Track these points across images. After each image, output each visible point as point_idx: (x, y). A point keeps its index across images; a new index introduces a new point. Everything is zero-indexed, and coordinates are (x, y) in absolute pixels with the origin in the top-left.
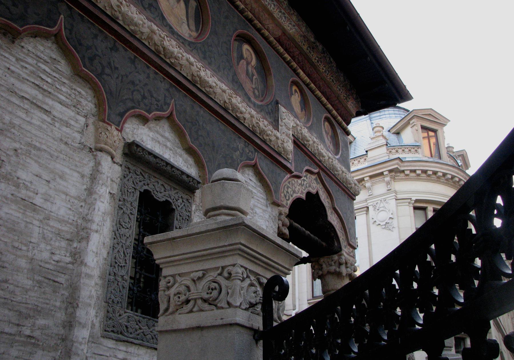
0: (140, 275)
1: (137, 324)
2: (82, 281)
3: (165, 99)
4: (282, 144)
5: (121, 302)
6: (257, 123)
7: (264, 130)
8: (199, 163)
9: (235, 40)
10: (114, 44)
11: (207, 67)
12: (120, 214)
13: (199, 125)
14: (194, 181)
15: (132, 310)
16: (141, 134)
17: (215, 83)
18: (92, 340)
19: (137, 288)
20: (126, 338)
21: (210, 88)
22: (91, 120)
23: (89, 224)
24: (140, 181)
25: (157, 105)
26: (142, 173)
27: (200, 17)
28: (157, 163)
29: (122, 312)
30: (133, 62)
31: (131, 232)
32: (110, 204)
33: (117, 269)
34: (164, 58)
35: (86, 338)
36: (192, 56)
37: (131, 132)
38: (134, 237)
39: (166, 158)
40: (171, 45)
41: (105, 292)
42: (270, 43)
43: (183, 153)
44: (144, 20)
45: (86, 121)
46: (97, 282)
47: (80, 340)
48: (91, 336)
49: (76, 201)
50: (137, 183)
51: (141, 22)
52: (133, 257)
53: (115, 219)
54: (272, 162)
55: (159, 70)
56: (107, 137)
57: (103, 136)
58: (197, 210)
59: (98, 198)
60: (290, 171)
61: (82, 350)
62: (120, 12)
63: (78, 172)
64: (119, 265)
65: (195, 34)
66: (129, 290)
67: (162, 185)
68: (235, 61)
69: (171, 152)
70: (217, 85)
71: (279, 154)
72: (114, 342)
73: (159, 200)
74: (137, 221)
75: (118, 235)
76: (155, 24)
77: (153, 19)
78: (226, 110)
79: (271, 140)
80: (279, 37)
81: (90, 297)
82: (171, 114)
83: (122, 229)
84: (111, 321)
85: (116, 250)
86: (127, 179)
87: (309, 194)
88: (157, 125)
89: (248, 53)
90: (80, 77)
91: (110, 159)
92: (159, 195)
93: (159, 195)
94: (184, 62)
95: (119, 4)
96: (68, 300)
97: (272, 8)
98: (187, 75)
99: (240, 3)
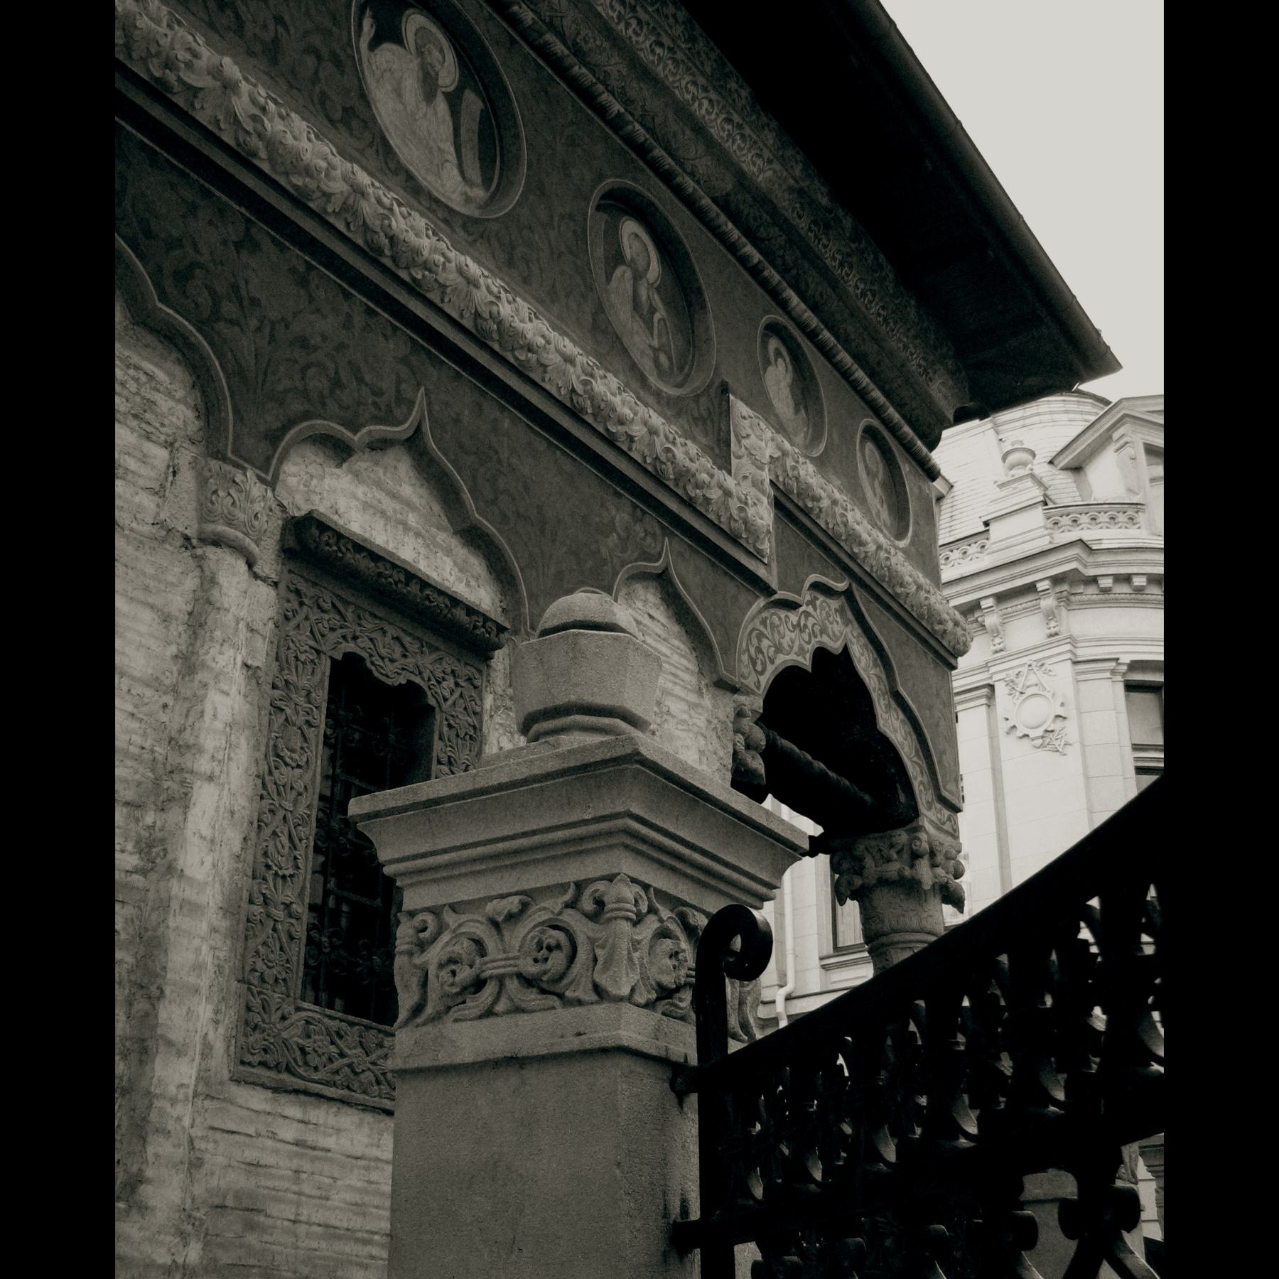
0: (339, 901)
1: (332, 1043)
2: (172, 922)
3: (398, 391)
4: (741, 509)
5: (284, 980)
6: (668, 450)
7: (688, 471)
9: (599, 208)
10: (248, 230)
11: (518, 289)
12: (275, 727)
13: (499, 461)
14: (489, 624)
15: (316, 1003)
16: (334, 491)
17: (543, 336)
18: (207, 1090)
19: (330, 938)
20: (300, 1084)
21: (530, 350)
22: (186, 456)
23: (188, 756)
24: (332, 629)
25: (375, 404)
26: (339, 605)
27: (492, 144)
28: (380, 574)
29: (288, 1008)
30: (303, 282)
31: (308, 776)
32: (245, 696)
33: (271, 883)
34: (393, 268)
35: (188, 1086)
36: (475, 260)
37: (302, 487)
38: (317, 791)
39: (404, 561)
40: (412, 228)
41: (240, 951)
42: (700, 214)
43: (455, 543)
44: (330, 157)
45: (172, 458)
46: (216, 923)
47: (172, 1090)
48: (203, 1078)
49: (148, 692)
50: (323, 636)
51: (323, 164)
52: (317, 850)
53: (264, 741)
54: (713, 564)
55: (377, 303)
56: (234, 503)
57: (223, 501)
58: (498, 708)
59: (212, 683)
60: (766, 590)
61: (179, 1119)
62: (260, 136)
63: (152, 607)
64: (276, 874)
65: (479, 193)
66: (307, 945)
68: (599, 270)
69: (420, 540)
70: (548, 342)
71: (734, 540)
72: (269, 1094)
73: (389, 682)
74: (325, 744)
75: (271, 787)
76: (364, 168)
77: (357, 154)
78: (575, 414)
79: (707, 501)
80: (728, 195)
81: (198, 967)
82: (418, 430)
83: (284, 769)
84: (257, 1035)
85: (267, 832)
86: (293, 623)
88: (377, 464)
89: (636, 245)
90: (152, 330)
91: (242, 566)
92: (389, 668)
93: (389, 668)
94: (450, 277)
95: (257, 112)
96: (133, 978)
97: (703, 112)
98: (462, 316)
99: (611, 98)
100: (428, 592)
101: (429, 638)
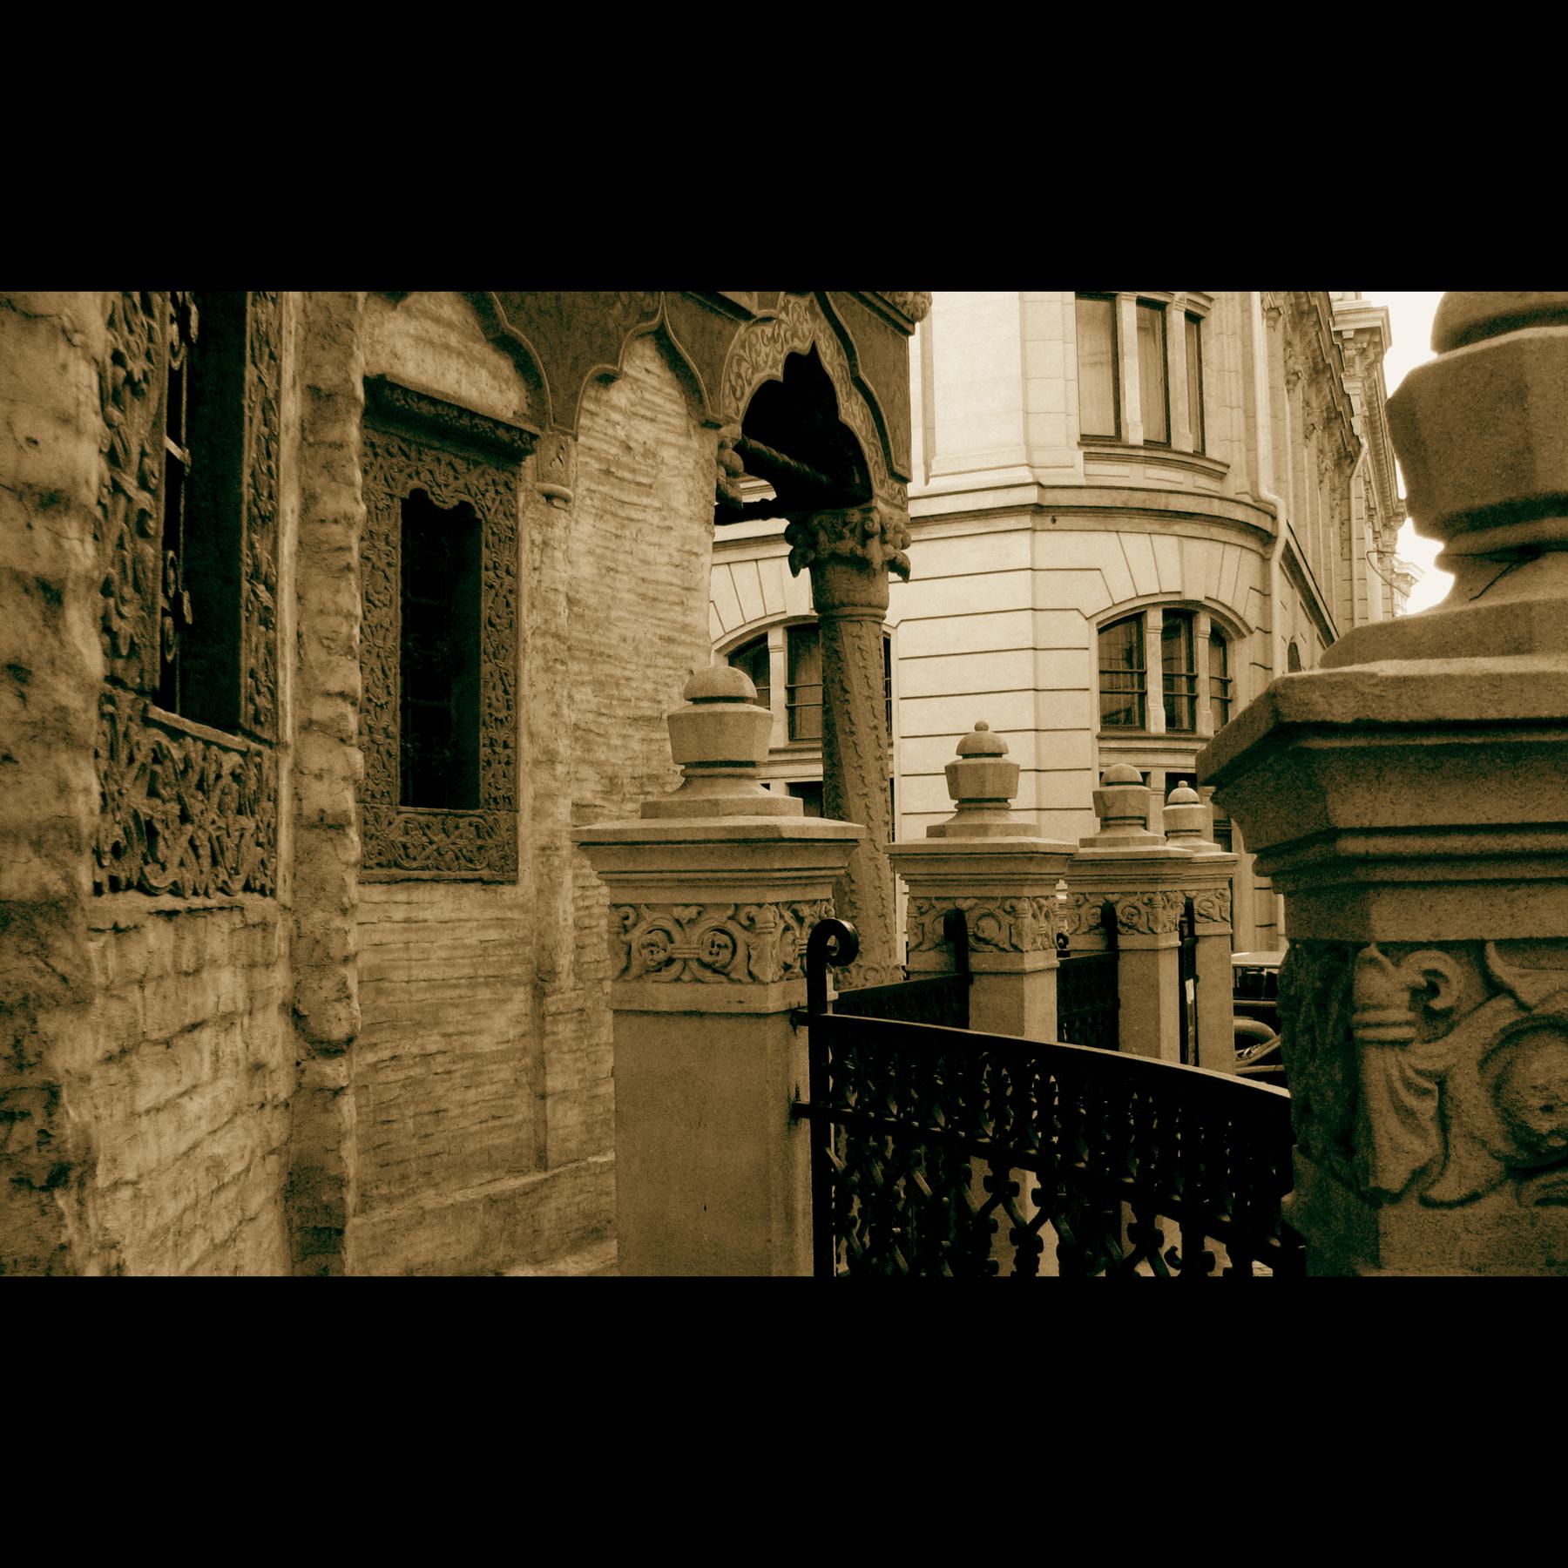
8: (525, 368)
31: (391, 613)
67: (450, 464)
73: (446, 507)
93: (445, 492)
101: (474, 455)
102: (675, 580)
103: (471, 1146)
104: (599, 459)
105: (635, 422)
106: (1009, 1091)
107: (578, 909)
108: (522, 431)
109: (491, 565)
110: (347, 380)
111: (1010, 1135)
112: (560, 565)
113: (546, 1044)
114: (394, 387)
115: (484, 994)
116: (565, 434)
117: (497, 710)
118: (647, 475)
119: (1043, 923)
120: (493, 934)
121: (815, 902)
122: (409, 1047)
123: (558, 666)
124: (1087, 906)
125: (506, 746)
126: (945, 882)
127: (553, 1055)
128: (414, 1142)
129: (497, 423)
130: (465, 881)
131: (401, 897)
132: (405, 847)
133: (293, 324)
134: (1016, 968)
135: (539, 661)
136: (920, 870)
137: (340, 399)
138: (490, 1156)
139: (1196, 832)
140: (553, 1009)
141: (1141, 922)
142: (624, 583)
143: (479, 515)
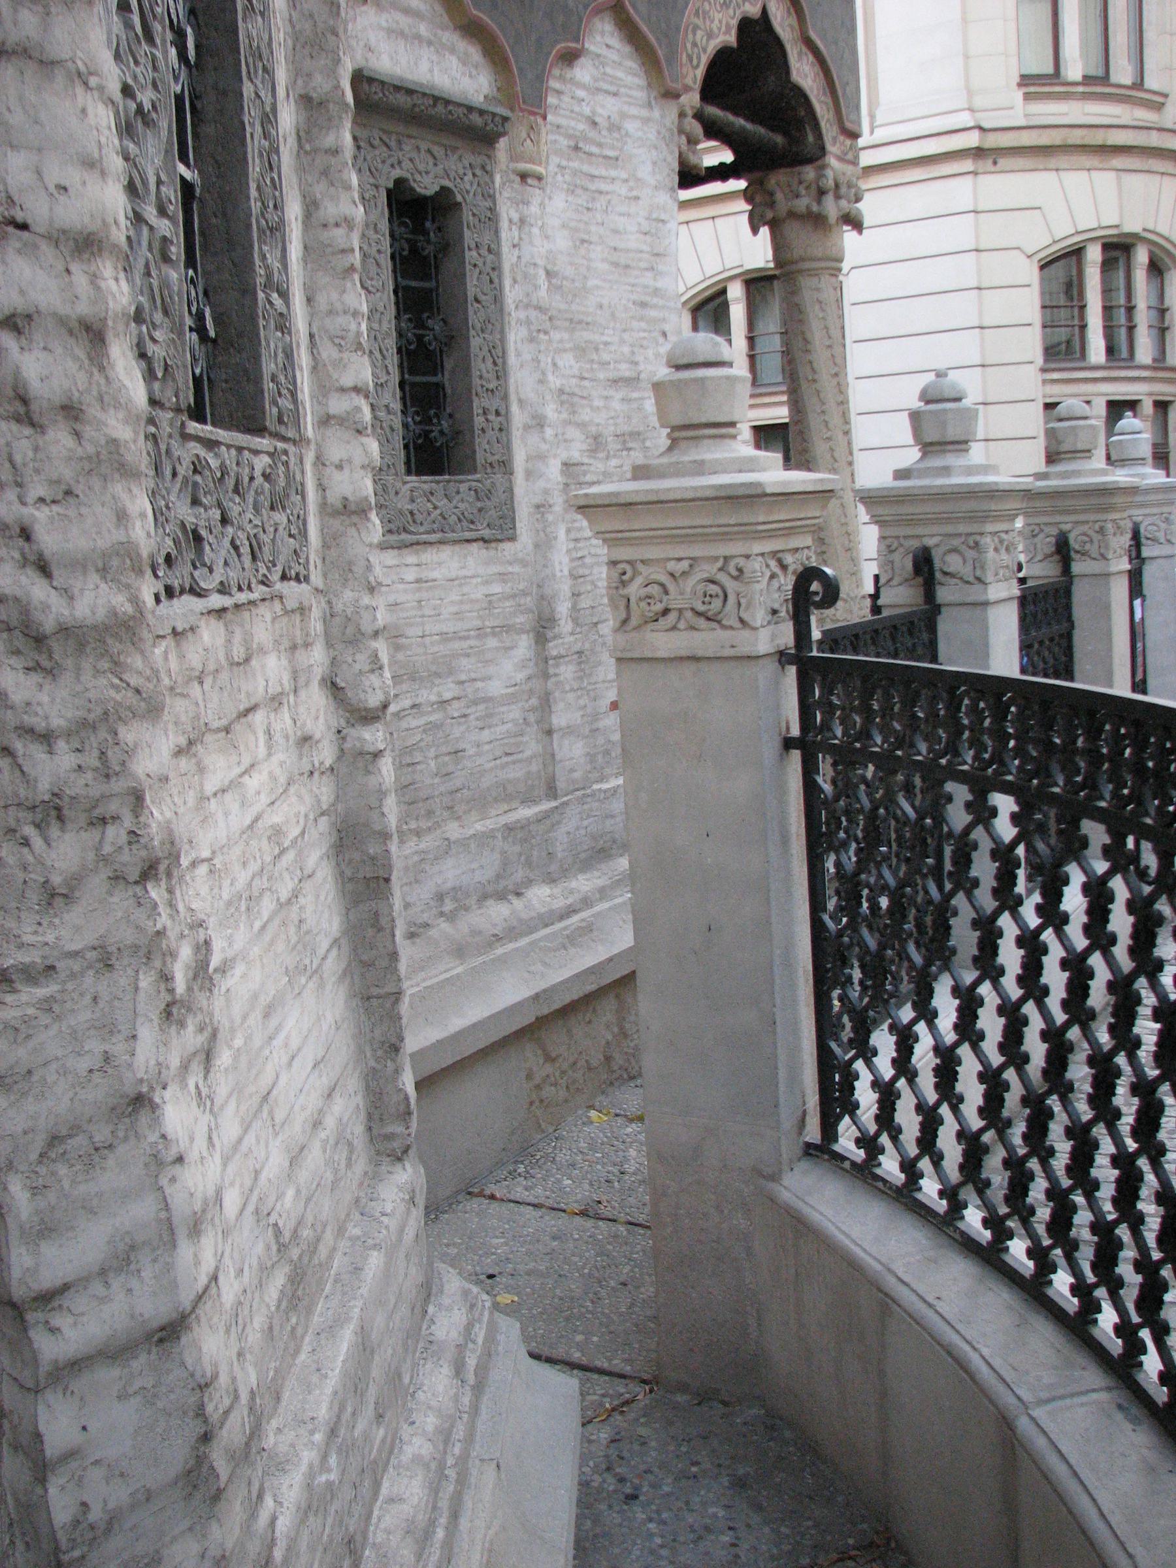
31: (385, 296)
87: (745, 25)
100: (450, 107)
102: (645, 248)
103: (486, 782)
104: (570, 137)
105: (600, 97)
106: (987, 723)
107: (572, 560)
108: (494, 115)
109: (473, 246)
110: (337, 87)
111: (990, 763)
112: (537, 241)
113: (550, 684)
114: (371, 80)
115: (492, 643)
116: (534, 114)
117: (489, 381)
118: (613, 148)
119: (1004, 556)
120: (496, 588)
121: (797, 550)
122: (427, 696)
123: (542, 336)
124: (1041, 536)
125: (498, 413)
126: (911, 522)
127: (557, 694)
128: (436, 780)
129: (470, 109)
130: (468, 541)
131: (411, 559)
132: (411, 513)
133: (282, 35)
134: (982, 598)
135: (523, 332)
136: (884, 511)
137: (331, 106)
138: (505, 789)
139: (1141, 460)
140: (554, 653)
141: (1094, 550)
142: (597, 252)
143: (459, 198)
